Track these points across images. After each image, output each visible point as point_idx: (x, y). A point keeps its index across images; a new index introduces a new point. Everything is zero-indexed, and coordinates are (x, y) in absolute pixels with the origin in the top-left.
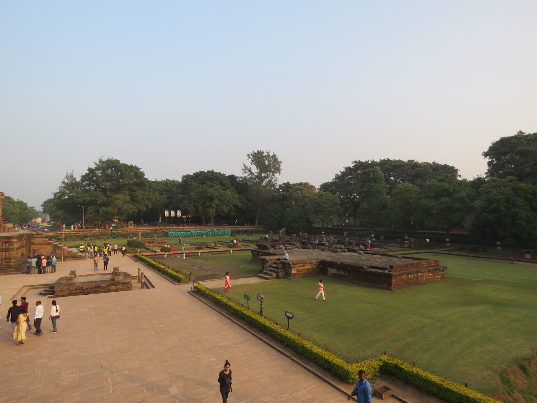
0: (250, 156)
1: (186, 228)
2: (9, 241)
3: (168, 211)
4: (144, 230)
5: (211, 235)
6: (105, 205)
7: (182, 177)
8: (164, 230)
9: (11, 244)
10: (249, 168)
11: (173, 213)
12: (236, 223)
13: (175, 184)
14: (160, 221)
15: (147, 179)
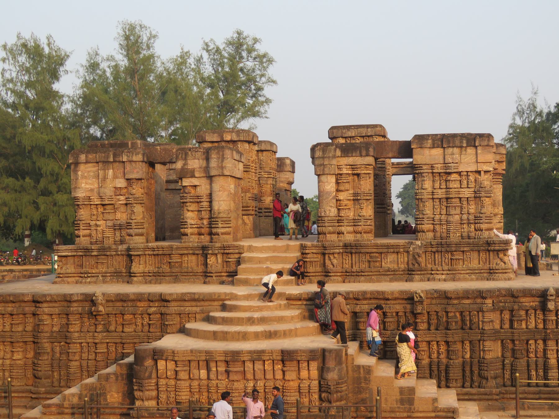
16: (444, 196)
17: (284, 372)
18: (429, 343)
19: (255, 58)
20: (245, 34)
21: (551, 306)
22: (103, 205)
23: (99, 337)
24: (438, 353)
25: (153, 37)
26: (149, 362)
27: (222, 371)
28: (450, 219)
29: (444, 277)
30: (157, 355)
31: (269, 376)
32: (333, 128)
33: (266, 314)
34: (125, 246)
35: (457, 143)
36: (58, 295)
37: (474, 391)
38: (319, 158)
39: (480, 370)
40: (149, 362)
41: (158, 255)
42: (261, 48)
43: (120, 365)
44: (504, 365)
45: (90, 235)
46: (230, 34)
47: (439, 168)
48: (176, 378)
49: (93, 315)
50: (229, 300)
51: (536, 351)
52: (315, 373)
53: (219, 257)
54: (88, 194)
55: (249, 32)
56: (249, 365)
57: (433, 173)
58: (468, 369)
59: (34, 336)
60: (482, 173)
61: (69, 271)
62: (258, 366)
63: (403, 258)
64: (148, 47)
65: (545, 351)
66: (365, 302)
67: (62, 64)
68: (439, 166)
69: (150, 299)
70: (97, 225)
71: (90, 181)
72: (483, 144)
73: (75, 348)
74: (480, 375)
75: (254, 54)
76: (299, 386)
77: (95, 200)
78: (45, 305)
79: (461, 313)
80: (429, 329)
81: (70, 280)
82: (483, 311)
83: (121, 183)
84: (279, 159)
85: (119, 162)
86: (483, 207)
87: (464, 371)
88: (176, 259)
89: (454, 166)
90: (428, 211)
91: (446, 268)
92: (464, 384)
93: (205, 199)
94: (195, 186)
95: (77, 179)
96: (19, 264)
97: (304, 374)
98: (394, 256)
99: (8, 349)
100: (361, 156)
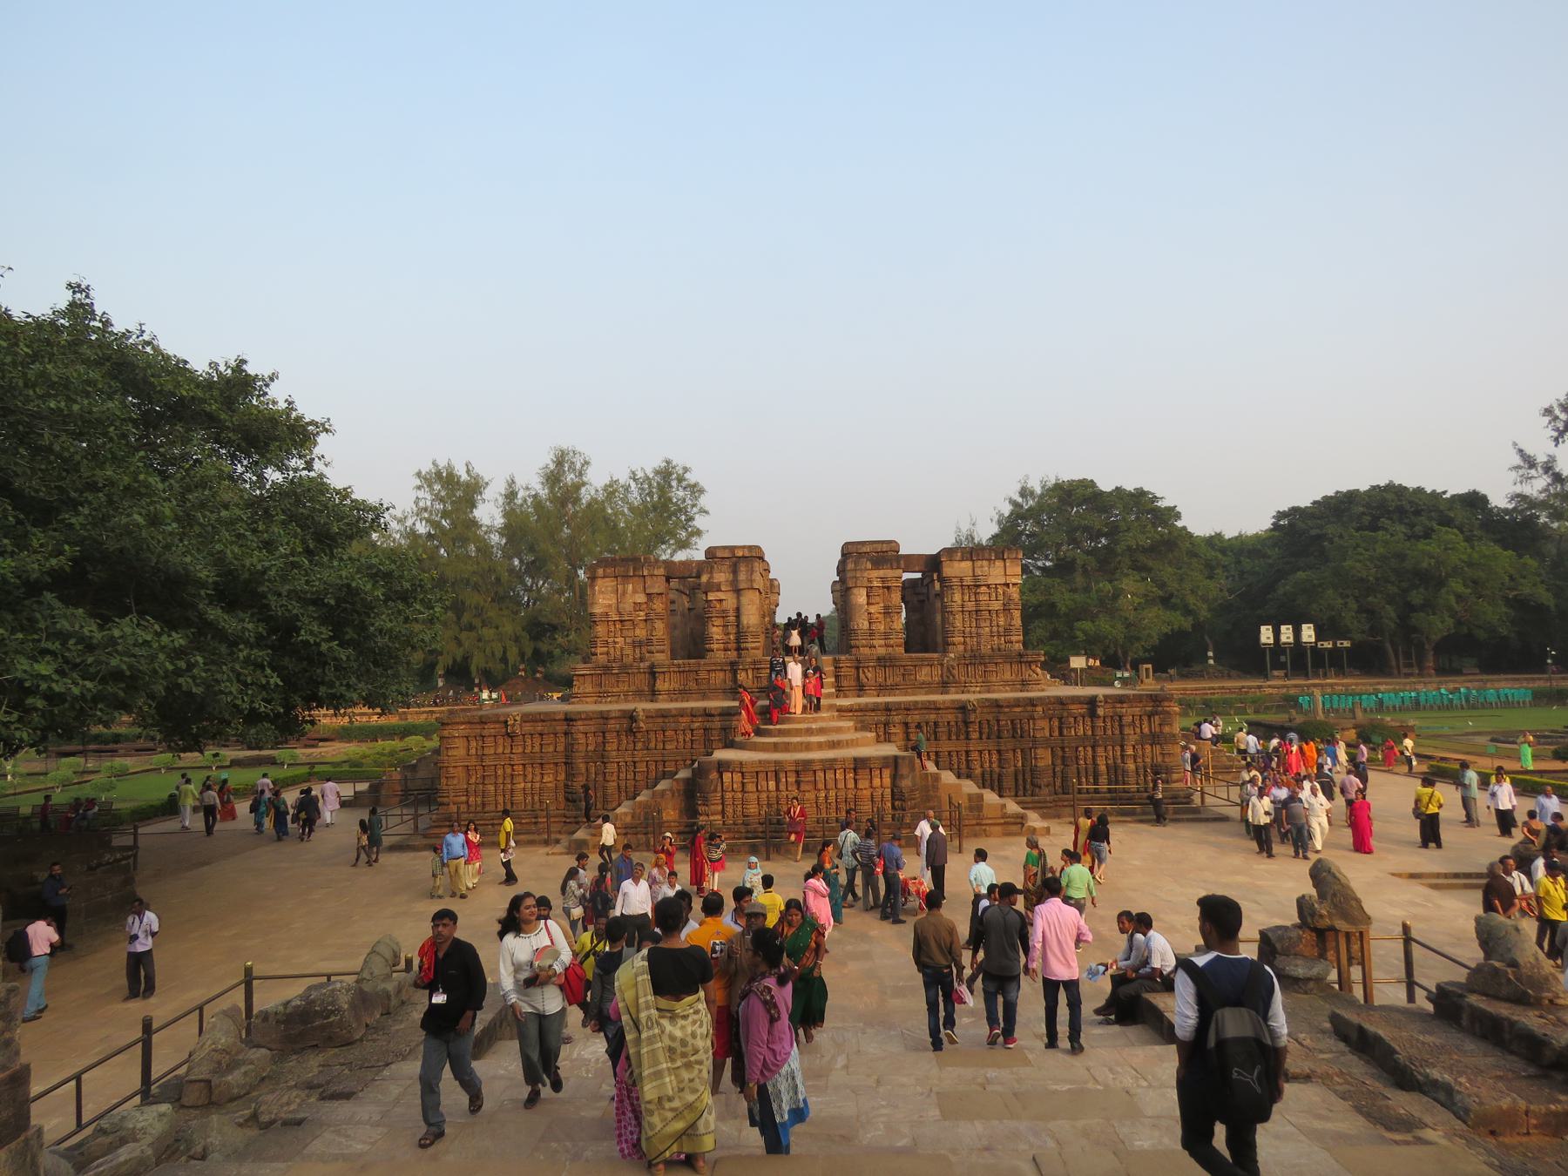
0: (1557, 412)
1: (1343, 685)
2: (1160, 709)
3: (1270, 627)
4: (1204, 689)
5: (1456, 706)
6: (1081, 613)
7: (1274, 517)
8: (1271, 690)
9: (1167, 718)
10: (1541, 458)
11: (1287, 634)
12: (1549, 661)
13: (1225, 544)
14: (1211, 662)
15: (1184, 528)
17: (856, 781)
18: (981, 752)
19: (685, 488)
20: (674, 463)
21: (1100, 712)
22: (621, 621)
23: (639, 755)
24: (990, 761)
25: (587, 463)
26: (714, 775)
28: (980, 631)
29: (978, 689)
30: (722, 766)
31: (841, 785)
32: (847, 544)
33: (823, 725)
34: (647, 664)
35: (987, 556)
36: (593, 712)
37: (1028, 799)
38: (851, 570)
39: (1033, 778)
40: (714, 775)
41: (683, 672)
42: (691, 478)
43: (677, 780)
44: (1054, 772)
45: (608, 653)
46: (658, 463)
47: (968, 581)
48: (743, 791)
49: (631, 732)
51: (1085, 759)
52: (887, 781)
53: (750, 672)
54: (606, 610)
55: (679, 461)
56: (820, 775)
57: (962, 586)
58: (1020, 778)
59: (567, 757)
61: (587, 691)
62: (830, 775)
63: (937, 671)
64: (581, 474)
65: (1094, 757)
66: (916, 712)
67: (481, 493)
69: (693, 714)
70: (615, 643)
72: (1011, 556)
73: (612, 768)
74: (1032, 784)
75: (684, 484)
76: (872, 795)
78: (580, 723)
79: (1012, 721)
80: (981, 738)
81: (588, 699)
82: (1034, 719)
83: (641, 598)
84: (772, 580)
85: (639, 576)
86: (1012, 619)
87: (1016, 780)
88: (703, 675)
90: (958, 624)
91: (980, 680)
92: (1017, 792)
93: (731, 613)
94: (721, 600)
95: (594, 594)
96: (436, 704)
97: (877, 782)
98: (929, 668)
99: (538, 771)
100: (892, 569)
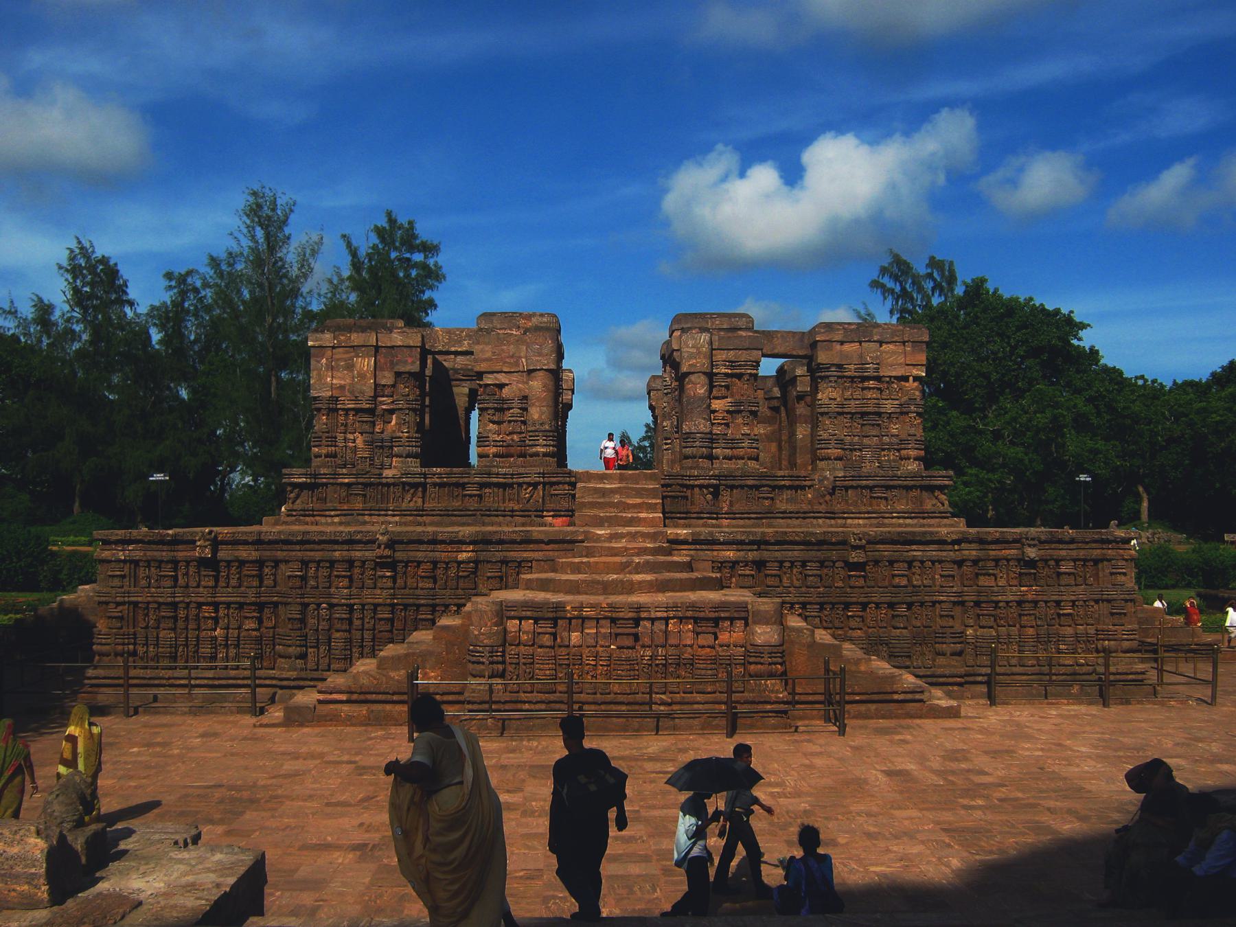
16: (859, 410)
27: (605, 633)
47: (851, 371)
50: (582, 541)
54: (336, 393)
60: (911, 378)
68: (852, 367)
71: (339, 374)
77: (347, 402)
81: (308, 519)
89: (875, 369)
